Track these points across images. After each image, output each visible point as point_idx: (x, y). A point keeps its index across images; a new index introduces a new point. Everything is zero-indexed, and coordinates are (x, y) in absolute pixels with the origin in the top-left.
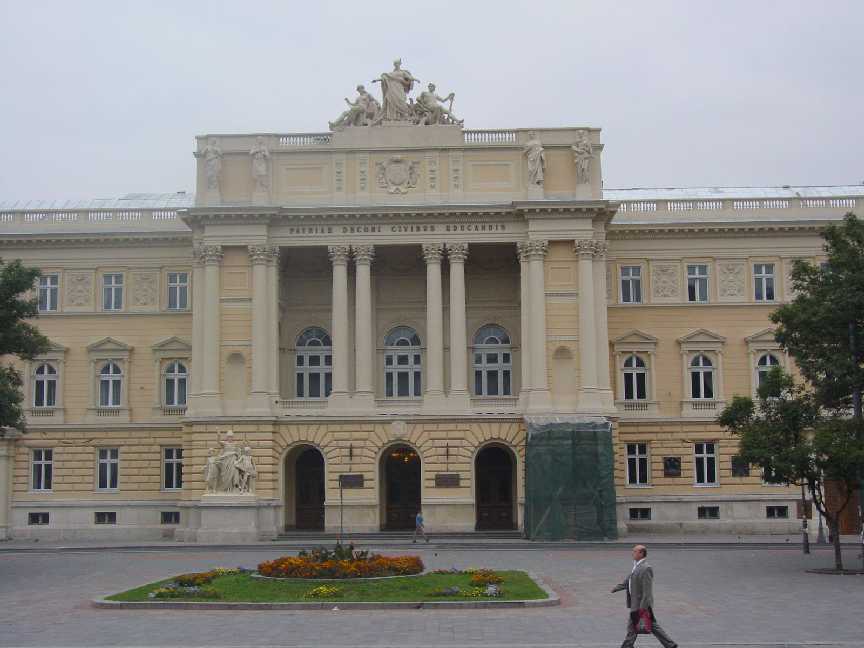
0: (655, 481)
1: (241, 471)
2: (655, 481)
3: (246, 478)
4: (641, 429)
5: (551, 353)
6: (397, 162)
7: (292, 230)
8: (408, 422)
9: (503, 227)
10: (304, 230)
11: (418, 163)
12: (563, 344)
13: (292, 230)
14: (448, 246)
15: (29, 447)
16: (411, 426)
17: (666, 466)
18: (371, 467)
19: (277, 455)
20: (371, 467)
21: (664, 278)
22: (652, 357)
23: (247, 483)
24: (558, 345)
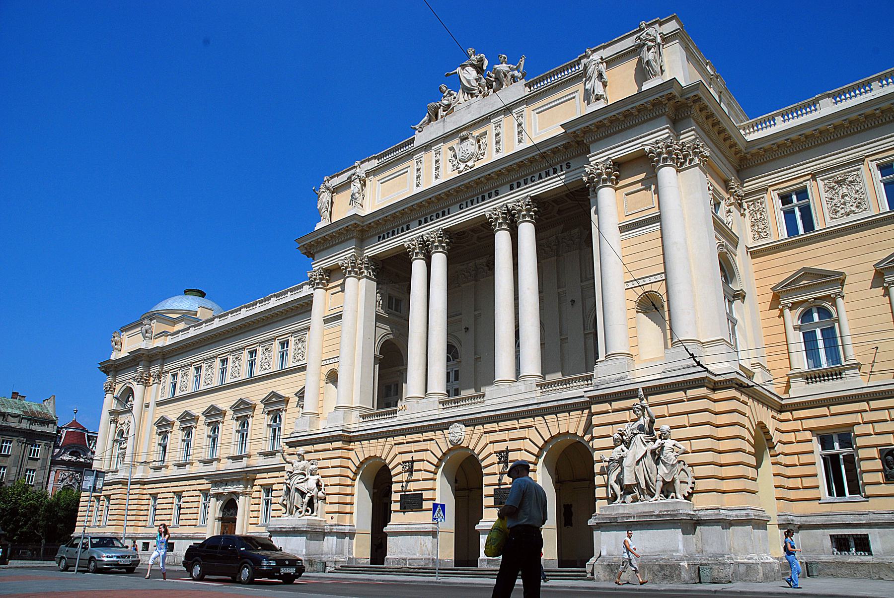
0: (869, 490)
1: (303, 494)
2: (869, 490)
3: (307, 499)
4: (835, 409)
5: (633, 305)
6: (464, 139)
7: (380, 237)
8: (467, 423)
9: (568, 166)
10: (388, 234)
11: (486, 133)
12: (647, 288)
13: (380, 237)
14: (510, 206)
15: (261, 485)
16: (471, 428)
17: (885, 462)
18: (429, 484)
19: (351, 475)
20: (429, 484)
21: (844, 190)
22: (840, 301)
23: (311, 503)
24: (640, 291)
